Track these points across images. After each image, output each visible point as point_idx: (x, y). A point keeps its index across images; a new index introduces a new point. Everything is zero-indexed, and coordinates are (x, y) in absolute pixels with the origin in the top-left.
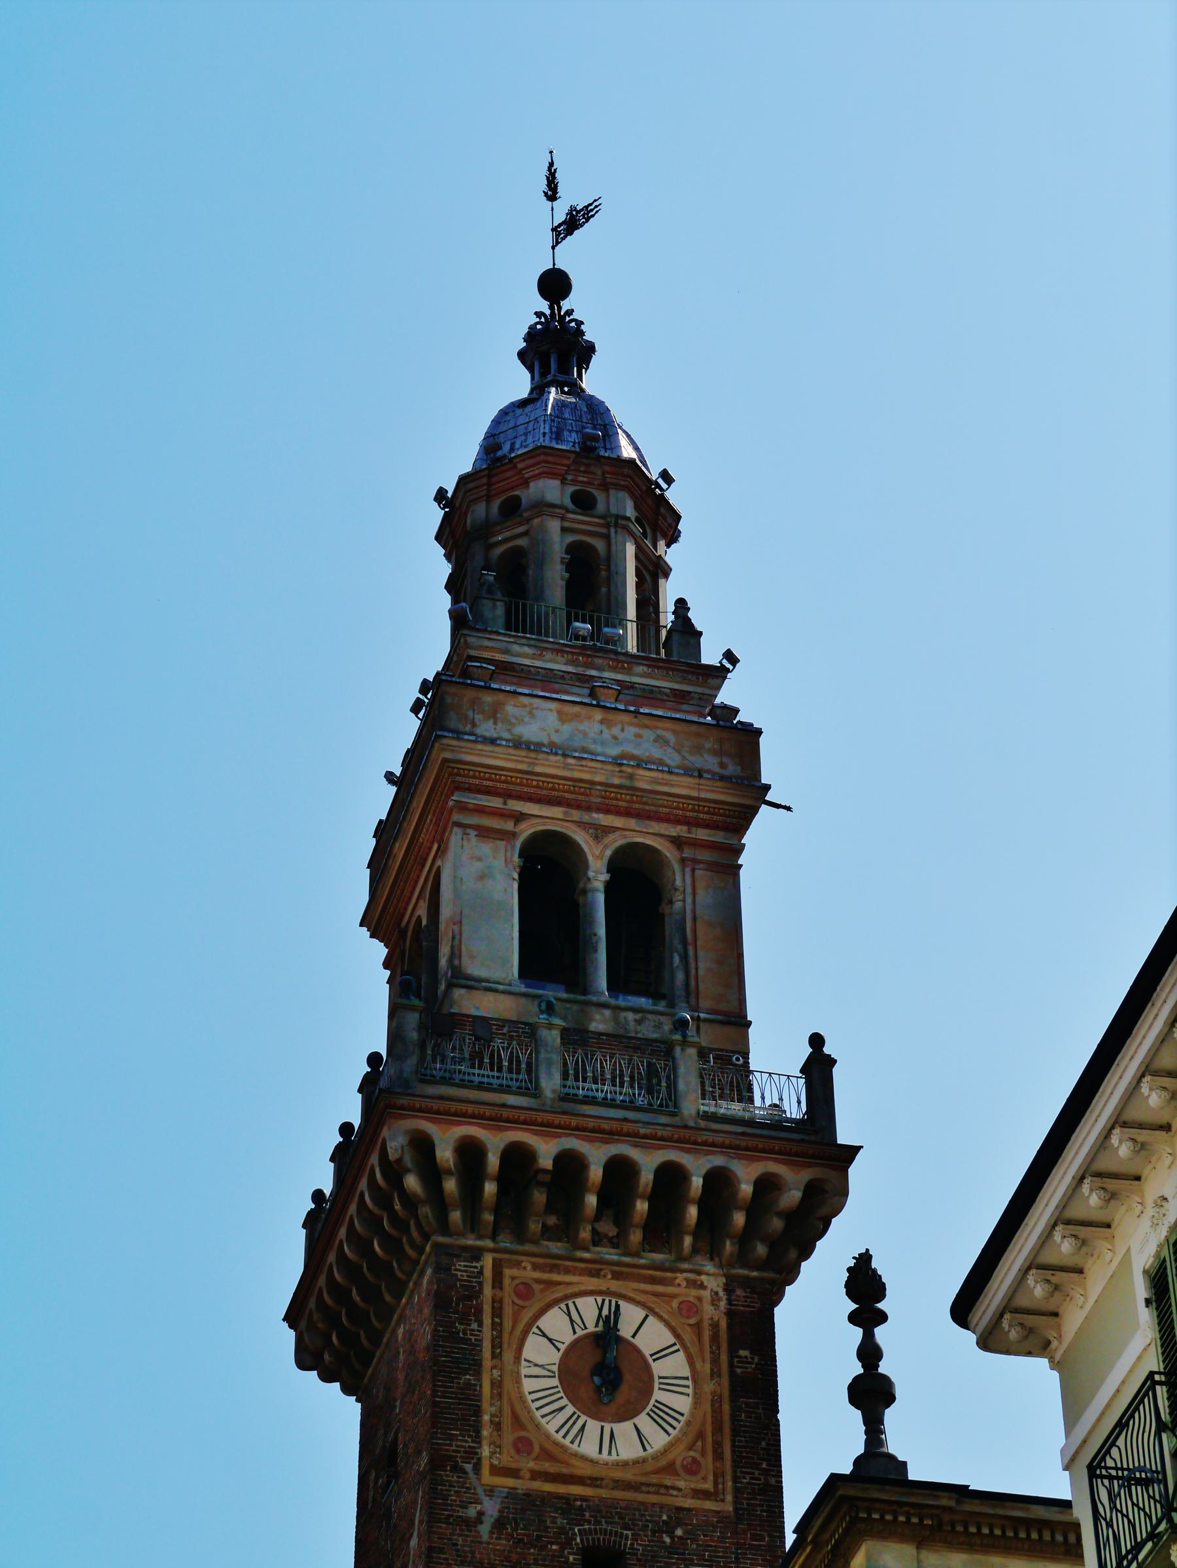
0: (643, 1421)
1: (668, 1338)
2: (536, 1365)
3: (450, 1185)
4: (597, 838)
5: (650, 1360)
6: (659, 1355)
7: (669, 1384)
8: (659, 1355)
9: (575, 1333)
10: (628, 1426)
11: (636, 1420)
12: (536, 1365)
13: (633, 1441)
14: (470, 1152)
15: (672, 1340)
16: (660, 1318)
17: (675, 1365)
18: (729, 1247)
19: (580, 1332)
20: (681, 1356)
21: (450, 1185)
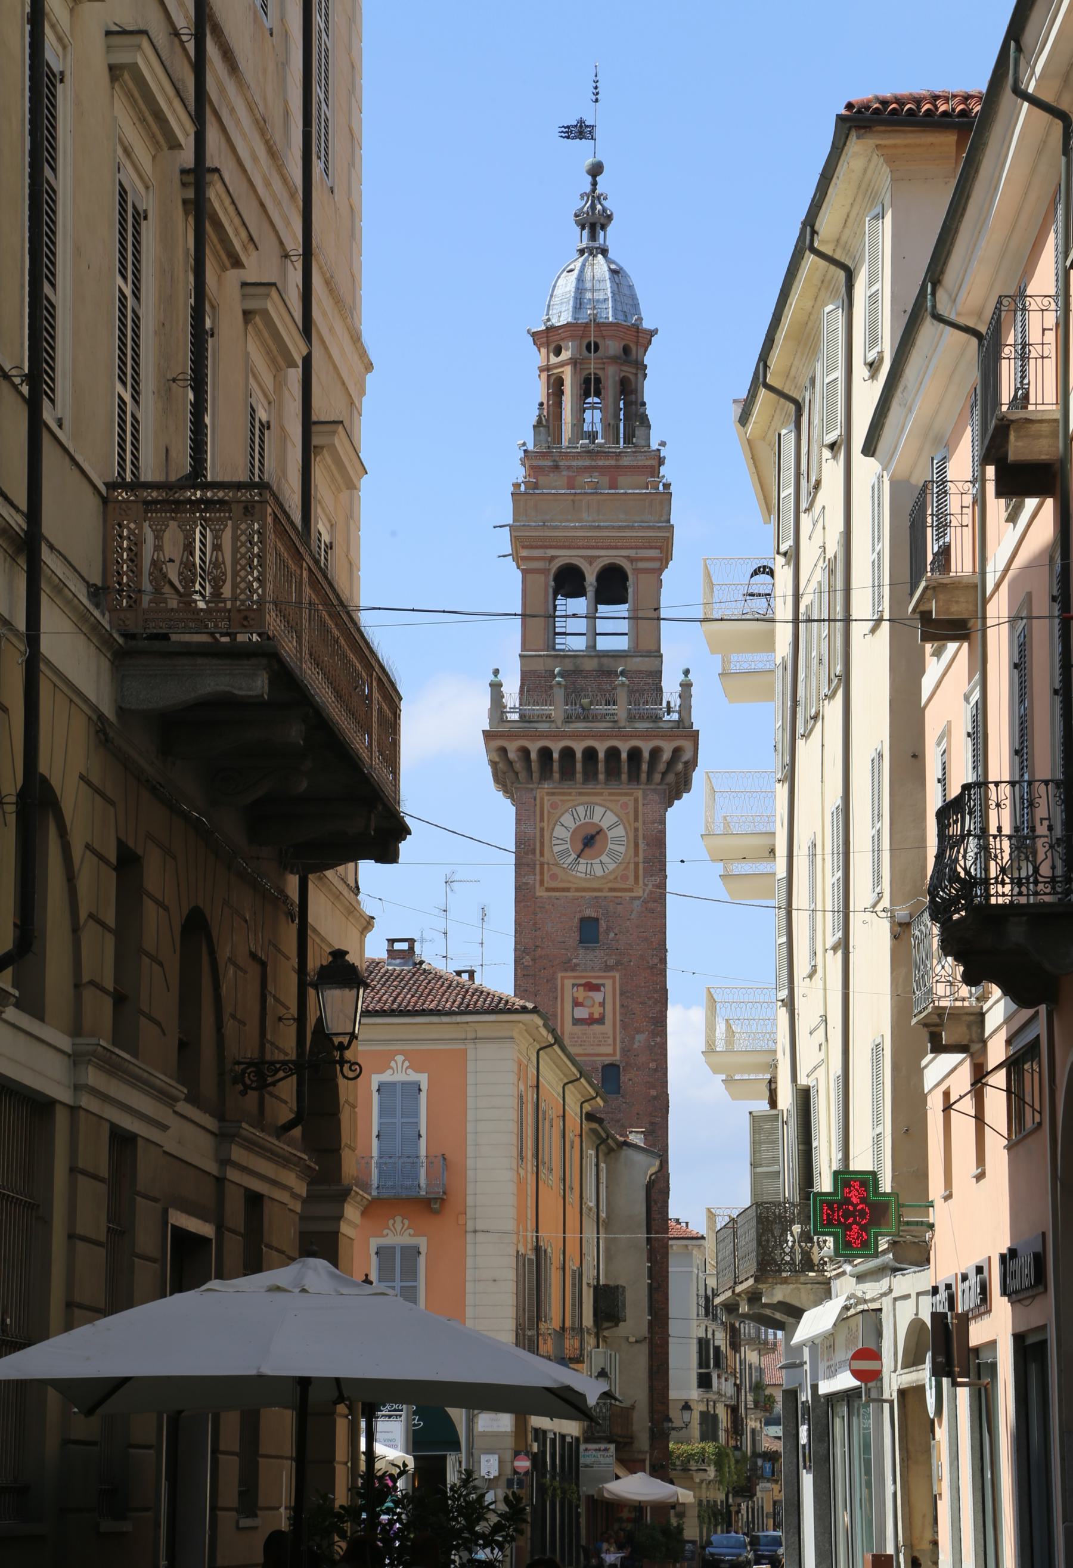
0: (604, 858)
1: (616, 819)
3: (518, 766)
4: (591, 564)
6: (610, 828)
7: (616, 840)
8: (610, 828)
10: (597, 861)
13: (600, 867)
14: (525, 752)
16: (612, 811)
17: (619, 831)
18: (644, 776)
19: (578, 823)
20: (621, 826)
21: (518, 766)
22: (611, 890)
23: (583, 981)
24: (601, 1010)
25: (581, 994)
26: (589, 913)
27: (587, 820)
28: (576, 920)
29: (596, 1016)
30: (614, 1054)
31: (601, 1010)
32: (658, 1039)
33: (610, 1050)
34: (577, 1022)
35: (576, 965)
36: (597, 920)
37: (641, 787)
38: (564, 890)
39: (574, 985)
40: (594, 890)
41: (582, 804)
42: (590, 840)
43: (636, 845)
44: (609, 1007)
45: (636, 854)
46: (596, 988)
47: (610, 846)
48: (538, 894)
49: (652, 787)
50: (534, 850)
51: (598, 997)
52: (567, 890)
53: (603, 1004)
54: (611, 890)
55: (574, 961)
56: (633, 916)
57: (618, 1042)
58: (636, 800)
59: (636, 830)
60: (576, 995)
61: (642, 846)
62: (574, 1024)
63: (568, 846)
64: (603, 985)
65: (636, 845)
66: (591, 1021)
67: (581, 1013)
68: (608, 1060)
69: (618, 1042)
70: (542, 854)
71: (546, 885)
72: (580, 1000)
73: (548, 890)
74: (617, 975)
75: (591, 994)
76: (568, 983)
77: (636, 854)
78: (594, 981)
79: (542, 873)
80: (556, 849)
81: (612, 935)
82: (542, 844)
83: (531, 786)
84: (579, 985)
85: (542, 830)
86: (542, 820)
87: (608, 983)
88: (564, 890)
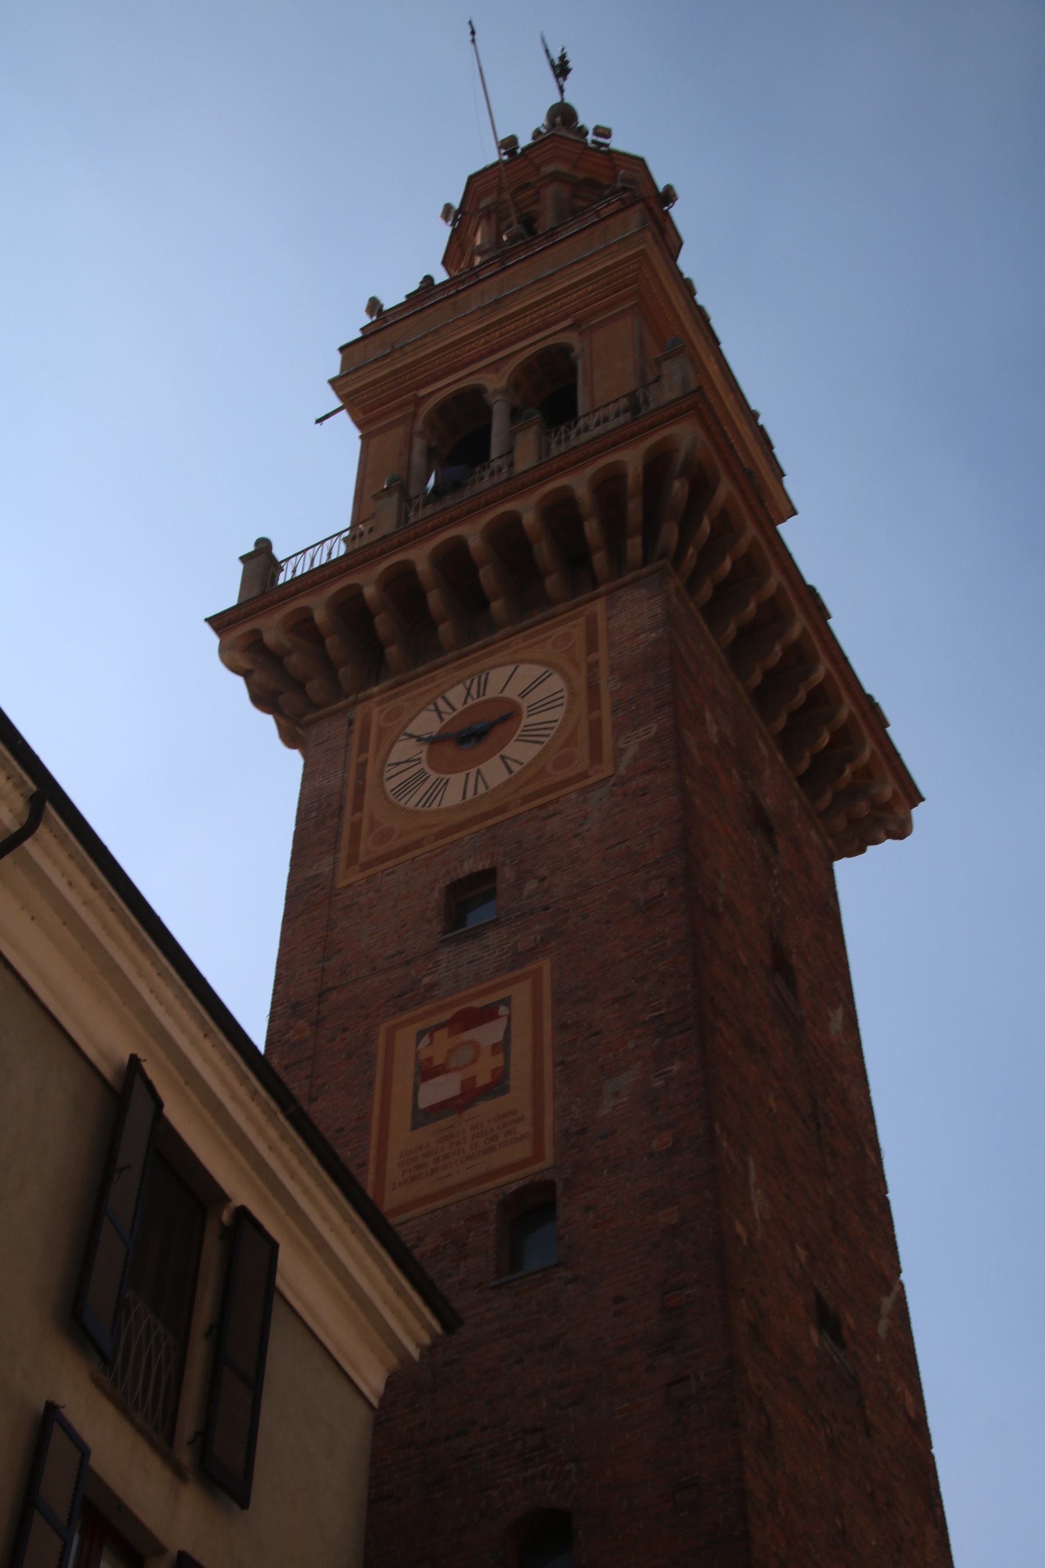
2: (398, 764)
5: (518, 699)
9: (442, 720)
11: (505, 752)
12: (398, 764)
15: (543, 669)
19: (447, 718)
22: (526, 800)
23: (448, 1015)
24: (499, 1060)
25: (440, 1046)
26: (469, 867)
27: (470, 702)
28: (436, 894)
29: (484, 1079)
30: (538, 1153)
31: (499, 1060)
32: (675, 1068)
33: (523, 1150)
34: (422, 1117)
35: (431, 987)
36: (490, 875)
37: (602, 589)
38: (405, 849)
39: (420, 1035)
40: (486, 816)
41: (462, 681)
42: (474, 735)
43: (593, 689)
44: (521, 1046)
45: (594, 704)
46: (489, 1014)
47: (525, 721)
48: (341, 883)
49: (627, 578)
50: (341, 808)
51: (489, 1034)
52: (417, 844)
53: (503, 1047)
54: (526, 800)
55: (425, 980)
56: (586, 827)
57: (548, 1119)
58: (592, 620)
59: (593, 667)
60: (424, 1055)
61: (606, 685)
62: (416, 1125)
63: (424, 765)
64: (506, 1002)
65: (593, 689)
66: (471, 1095)
67: (432, 1093)
68: (513, 1182)
69: (548, 1119)
70: (358, 806)
71: (363, 858)
72: (438, 1061)
73: (365, 866)
74: (546, 965)
75: (467, 1036)
76: (405, 1038)
77: (594, 704)
78: (478, 1003)
79: (355, 838)
80: (390, 785)
81: (531, 885)
82: (360, 791)
83: (342, 703)
84: (432, 1030)
85: (362, 766)
86: (363, 748)
87: (521, 994)
88: (405, 849)
